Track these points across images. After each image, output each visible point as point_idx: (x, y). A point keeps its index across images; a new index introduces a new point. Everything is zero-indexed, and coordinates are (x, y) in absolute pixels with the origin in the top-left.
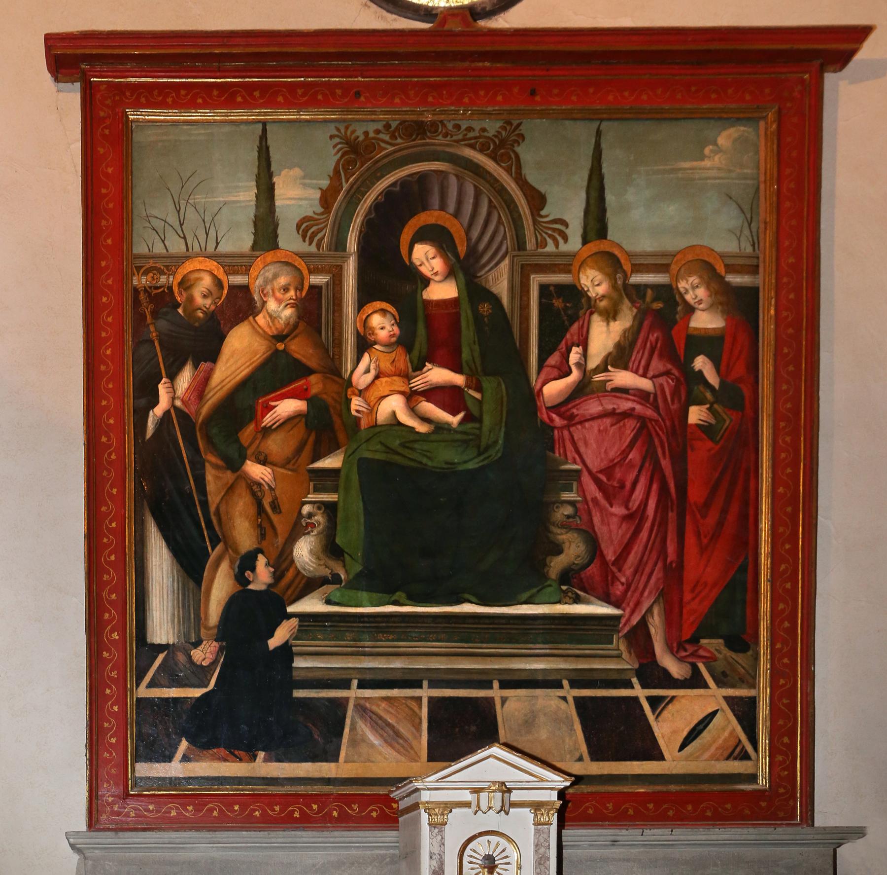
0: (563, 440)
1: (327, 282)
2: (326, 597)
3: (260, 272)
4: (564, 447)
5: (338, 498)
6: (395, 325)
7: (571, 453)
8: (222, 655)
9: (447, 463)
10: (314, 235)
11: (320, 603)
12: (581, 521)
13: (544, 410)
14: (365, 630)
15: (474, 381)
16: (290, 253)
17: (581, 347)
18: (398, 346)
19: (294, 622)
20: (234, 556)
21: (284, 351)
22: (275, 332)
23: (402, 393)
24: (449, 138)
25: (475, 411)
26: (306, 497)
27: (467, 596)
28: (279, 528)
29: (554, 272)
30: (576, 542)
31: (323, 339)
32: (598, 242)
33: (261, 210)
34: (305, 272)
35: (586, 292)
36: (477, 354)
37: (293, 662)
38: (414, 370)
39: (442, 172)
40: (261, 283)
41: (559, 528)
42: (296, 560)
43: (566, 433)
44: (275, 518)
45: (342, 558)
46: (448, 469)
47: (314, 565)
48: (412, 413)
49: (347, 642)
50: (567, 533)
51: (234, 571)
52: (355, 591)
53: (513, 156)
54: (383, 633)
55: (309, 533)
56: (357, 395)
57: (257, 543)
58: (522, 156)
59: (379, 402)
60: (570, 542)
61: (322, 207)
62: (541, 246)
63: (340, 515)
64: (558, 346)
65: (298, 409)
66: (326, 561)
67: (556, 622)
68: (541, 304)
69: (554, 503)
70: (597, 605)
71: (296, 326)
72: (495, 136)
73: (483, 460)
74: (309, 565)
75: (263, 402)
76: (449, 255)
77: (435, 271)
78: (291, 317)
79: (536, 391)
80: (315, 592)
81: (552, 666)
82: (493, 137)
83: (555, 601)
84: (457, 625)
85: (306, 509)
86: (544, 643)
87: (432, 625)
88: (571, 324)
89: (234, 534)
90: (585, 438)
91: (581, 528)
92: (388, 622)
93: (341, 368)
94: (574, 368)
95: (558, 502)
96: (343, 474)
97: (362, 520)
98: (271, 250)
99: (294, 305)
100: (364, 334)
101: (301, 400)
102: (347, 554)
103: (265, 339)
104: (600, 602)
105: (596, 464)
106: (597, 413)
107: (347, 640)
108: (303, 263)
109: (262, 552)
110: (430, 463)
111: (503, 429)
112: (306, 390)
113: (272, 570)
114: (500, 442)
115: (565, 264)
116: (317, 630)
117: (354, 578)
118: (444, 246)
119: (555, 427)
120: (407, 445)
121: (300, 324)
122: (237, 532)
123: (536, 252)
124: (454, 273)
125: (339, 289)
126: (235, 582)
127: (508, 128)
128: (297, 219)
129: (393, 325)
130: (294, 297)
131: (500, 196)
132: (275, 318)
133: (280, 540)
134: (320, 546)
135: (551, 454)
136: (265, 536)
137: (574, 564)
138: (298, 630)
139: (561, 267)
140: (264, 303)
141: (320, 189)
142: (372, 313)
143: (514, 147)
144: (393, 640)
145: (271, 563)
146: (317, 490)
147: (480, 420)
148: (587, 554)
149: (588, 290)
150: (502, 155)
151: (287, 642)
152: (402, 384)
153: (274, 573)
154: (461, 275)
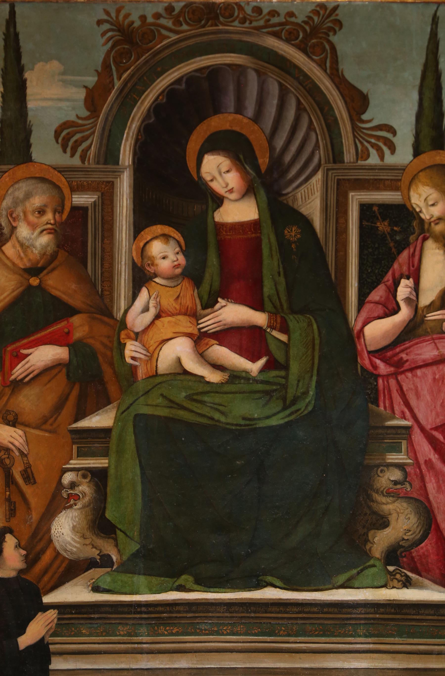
0: (390, 391)
1: (95, 202)
2: (94, 582)
3: (7, 191)
4: (391, 398)
5: (109, 463)
6: (181, 254)
7: (398, 406)
9: (244, 419)
10: (77, 144)
11: (86, 590)
12: (411, 488)
13: (366, 355)
14: (143, 622)
15: (279, 320)
16: (47, 167)
17: (411, 280)
18: (184, 279)
19: (52, 614)
21: (40, 287)
22: (28, 265)
23: (189, 335)
24: (247, 25)
25: (280, 356)
26: (68, 463)
27: (269, 579)
28: (33, 501)
29: (378, 189)
30: (406, 512)
31: (90, 274)
32: (434, 153)
33: (9, 113)
34: (66, 191)
35: (418, 213)
36: (282, 288)
37: (50, 664)
38: (204, 307)
39: (239, 66)
40: (9, 204)
41: (384, 496)
42: (54, 539)
43: (392, 382)
44: (27, 490)
45: (113, 535)
46: (245, 425)
47: (78, 545)
48: (201, 359)
49: (119, 638)
50: (394, 502)
52: (131, 575)
53: (327, 47)
54: (165, 625)
55: (71, 507)
56: (133, 339)
58: (339, 48)
59: (160, 346)
60: (398, 513)
61: (88, 109)
62: (362, 157)
63: (111, 484)
64: (383, 277)
65: (57, 357)
66: (92, 540)
67: (382, 610)
68: (361, 228)
69: (378, 466)
70: (433, 590)
71: (54, 257)
72: (305, 22)
73: (290, 415)
74: (70, 544)
75: (13, 350)
76: (248, 168)
77: (230, 187)
78: (47, 245)
79: (355, 332)
81: (377, 664)
82: (303, 24)
83: (380, 584)
84: (258, 615)
85: (68, 478)
86: (366, 636)
87: (226, 615)
88: (400, 252)
90: (416, 388)
91: (412, 496)
92: (171, 612)
93: (112, 307)
94: (403, 305)
95: (382, 466)
96: (114, 434)
97: (139, 488)
98: (23, 163)
99: (53, 231)
100: (142, 265)
101: (61, 346)
102: (121, 530)
103: (15, 273)
104: (437, 587)
105: (430, 420)
106: (432, 359)
107: (120, 635)
108: (63, 180)
109: (11, 532)
110: (223, 419)
111: (315, 378)
112: (68, 333)
113: (24, 552)
114: (311, 393)
115: (392, 180)
116: (81, 624)
117: (129, 559)
118: (241, 157)
119: (379, 376)
120: (195, 397)
121: (59, 253)
123: (357, 164)
124: (253, 189)
125: (110, 210)
127: (322, 12)
128: (55, 126)
129: (178, 253)
130: (52, 222)
131: (311, 96)
132: (28, 247)
133: (35, 516)
134: (85, 522)
135: (372, 406)
136: (15, 512)
137: (403, 539)
139: (387, 183)
140: (13, 229)
141: (85, 87)
142: (151, 240)
143: (329, 36)
144: (177, 634)
145: (23, 543)
146: (81, 454)
147: (286, 367)
148: (420, 527)
149: (421, 211)
150: (314, 46)
151: (43, 639)
152: (189, 325)
153: (26, 556)
154: (262, 193)
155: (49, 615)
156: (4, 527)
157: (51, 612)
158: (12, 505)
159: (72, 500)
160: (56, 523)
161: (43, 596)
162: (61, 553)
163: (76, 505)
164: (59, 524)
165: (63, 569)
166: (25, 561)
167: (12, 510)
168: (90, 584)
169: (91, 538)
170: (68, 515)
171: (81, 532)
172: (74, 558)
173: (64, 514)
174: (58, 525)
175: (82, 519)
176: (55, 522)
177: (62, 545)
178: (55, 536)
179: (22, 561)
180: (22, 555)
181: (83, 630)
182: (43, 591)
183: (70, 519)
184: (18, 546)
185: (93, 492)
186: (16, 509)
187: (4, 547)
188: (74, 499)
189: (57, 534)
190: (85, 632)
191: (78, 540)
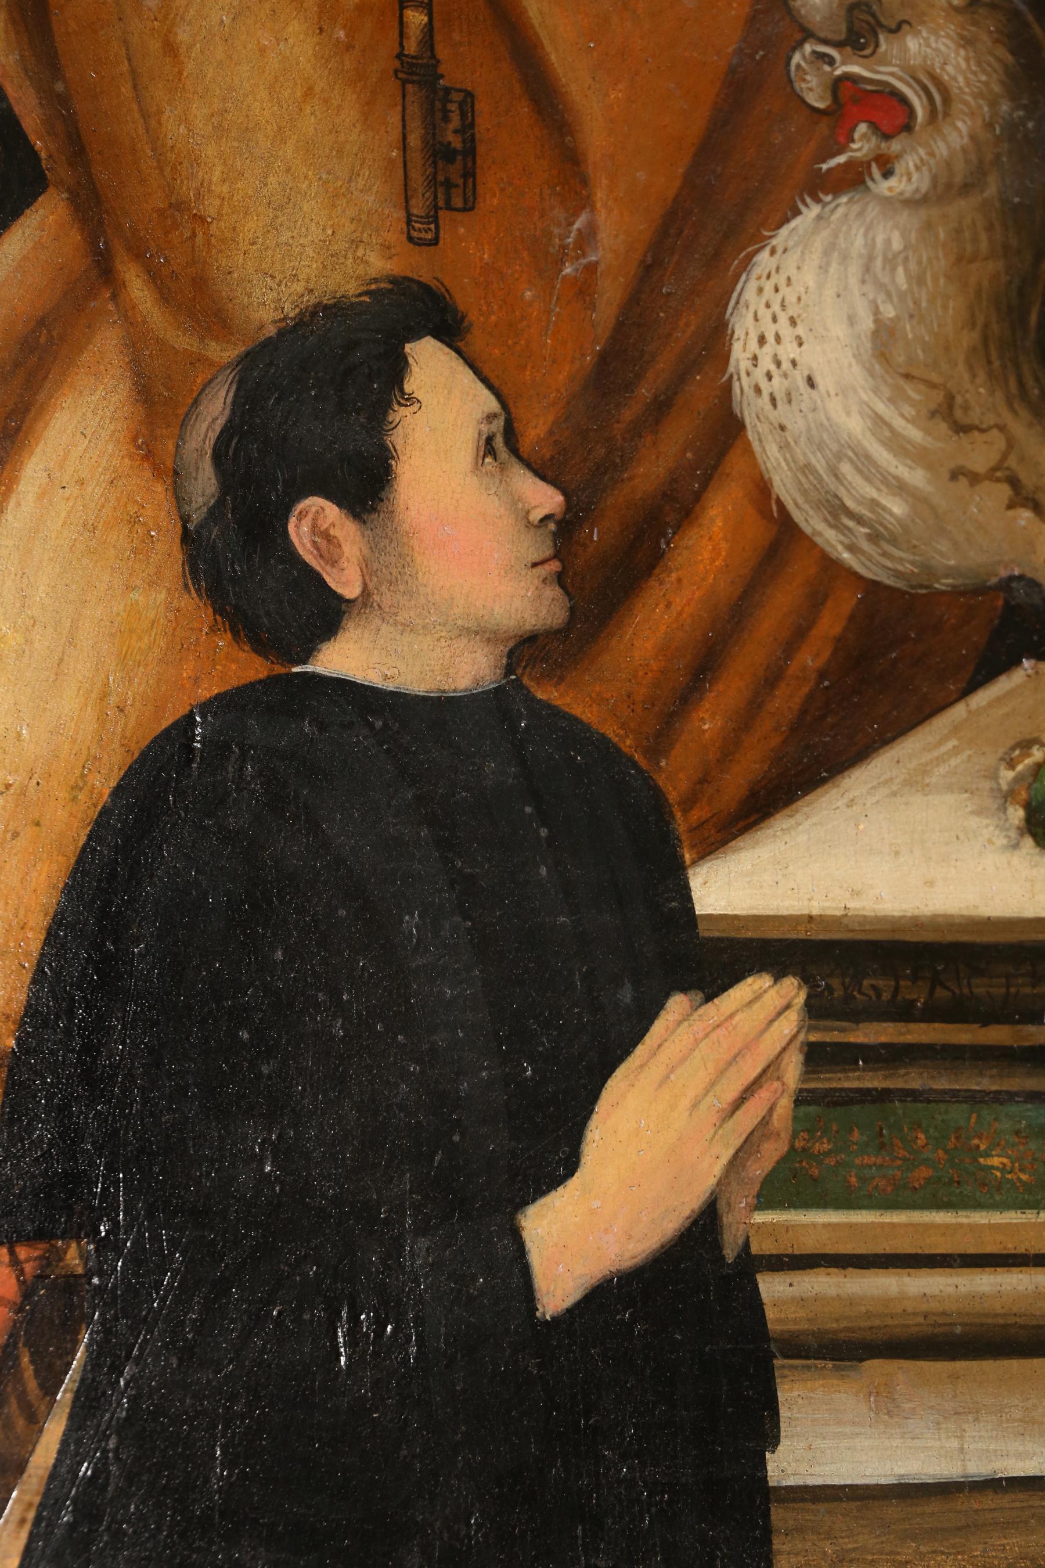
8: (50, 1389)
11: (986, 828)
20: (184, 341)
37: (773, 1440)
51: (179, 498)
57: (395, 236)
66: (1011, 443)
74: (865, 464)
80: (942, 722)
89: (173, 130)
116: (974, 1099)
122: (199, 112)
126: (191, 603)
136: (470, 174)
138: (802, 1099)
155: (748, 1022)
156: (394, 280)
157: (757, 998)
158: (446, 119)
159: (862, 128)
160: (760, 290)
161: (694, 863)
162: (808, 531)
163: (887, 174)
164: (783, 306)
165: (827, 654)
166: (555, 566)
167: (448, 154)
168: (1017, 779)
169: (1002, 428)
170: (841, 240)
171: (934, 377)
172: (898, 574)
173: (815, 231)
174: (776, 307)
175: (935, 279)
176: (752, 285)
177: (807, 468)
178: (758, 390)
179: (535, 565)
180: (536, 515)
181: (987, 1155)
182: (697, 815)
183: (854, 270)
184: (499, 442)
185: (997, 88)
186: (481, 149)
187: (396, 439)
188: (874, 126)
189: (769, 376)
190: (1003, 1169)
191: (915, 434)
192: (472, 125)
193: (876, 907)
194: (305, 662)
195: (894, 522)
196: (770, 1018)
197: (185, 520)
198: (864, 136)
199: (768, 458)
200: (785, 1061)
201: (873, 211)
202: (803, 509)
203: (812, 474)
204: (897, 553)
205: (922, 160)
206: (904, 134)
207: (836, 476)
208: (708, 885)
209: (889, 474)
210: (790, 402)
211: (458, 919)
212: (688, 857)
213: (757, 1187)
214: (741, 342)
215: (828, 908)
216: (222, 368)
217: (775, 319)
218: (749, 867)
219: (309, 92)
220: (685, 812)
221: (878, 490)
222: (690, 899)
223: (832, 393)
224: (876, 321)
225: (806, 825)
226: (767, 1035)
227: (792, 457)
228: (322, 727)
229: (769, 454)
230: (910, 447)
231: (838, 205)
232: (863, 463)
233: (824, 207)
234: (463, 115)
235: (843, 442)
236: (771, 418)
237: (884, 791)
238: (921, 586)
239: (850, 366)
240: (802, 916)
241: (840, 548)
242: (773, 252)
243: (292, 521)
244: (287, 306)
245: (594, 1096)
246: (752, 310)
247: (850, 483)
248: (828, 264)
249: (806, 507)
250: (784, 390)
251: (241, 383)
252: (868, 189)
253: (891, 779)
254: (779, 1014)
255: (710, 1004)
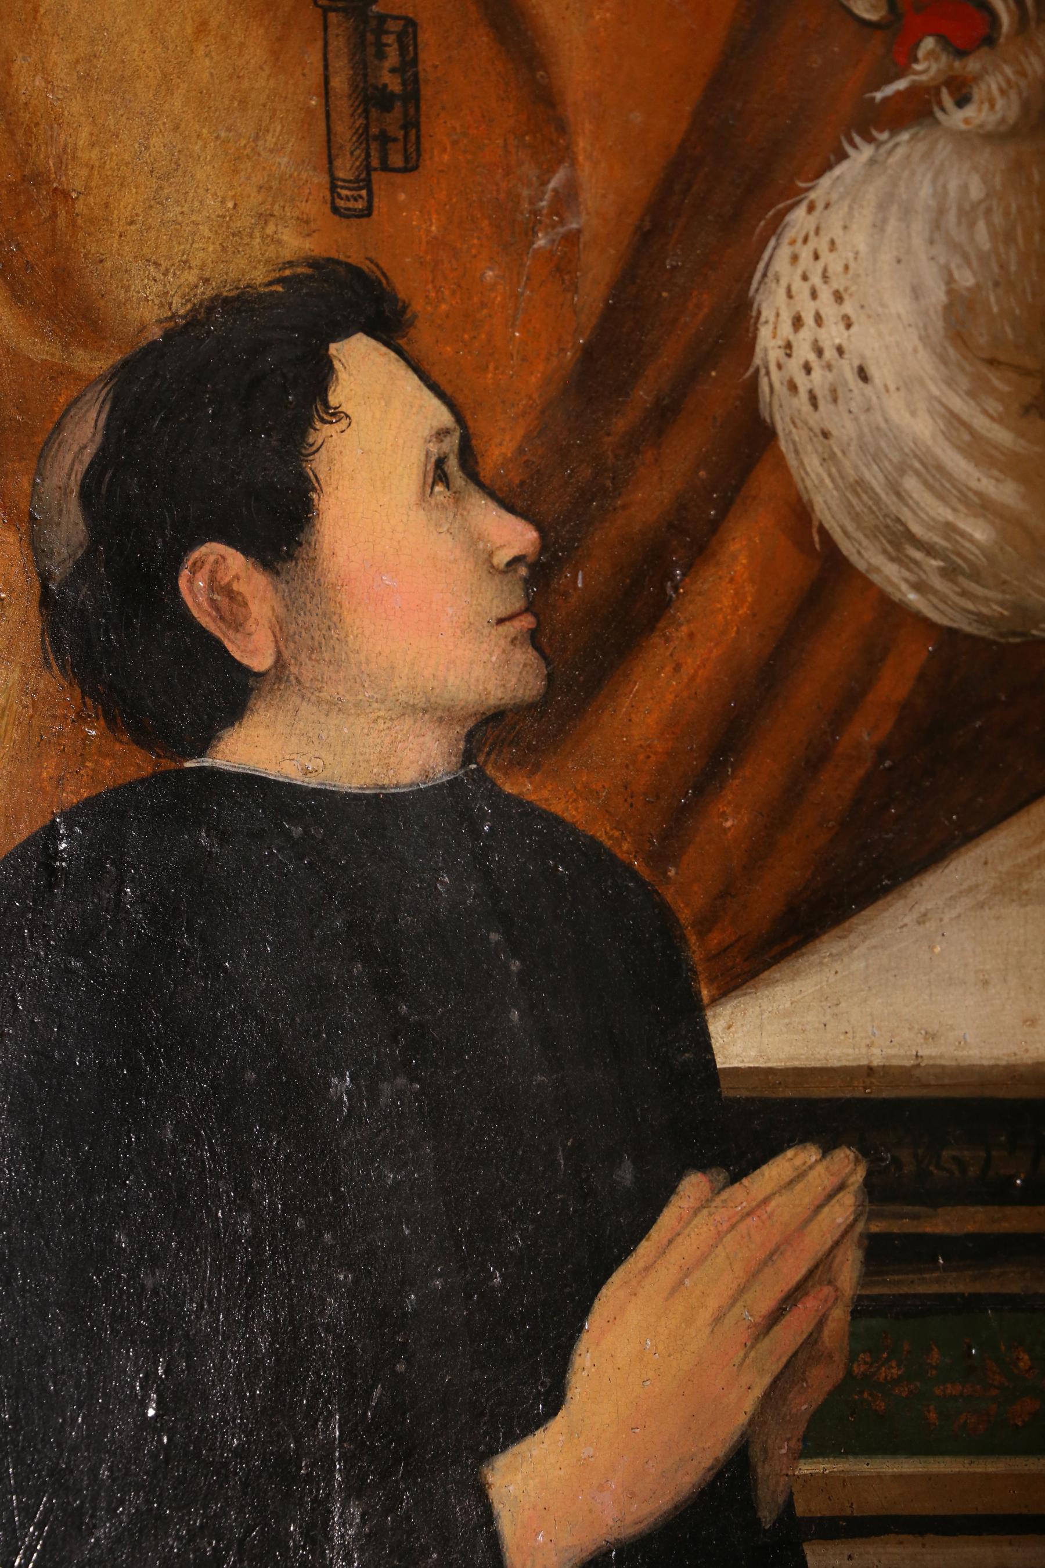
57: (315, 207)
122: (60, 59)
136: (412, 124)
156: (314, 263)
157: (800, 1176)
158: (381, 55)
159: (929, 43)
160: (795, 258)
161: (714, 1001)
162: (861, 566)
163: (962, 102)
164: (825, 277)
166: (527, 622)
167: (383, 100)
172: (981, 619)
174: (816, 279)
176: (784, 252)
177: (859, 486)
178: (793, 387)
179: (500, 621)
180: (502, 558)
182: (716, 939)
183: (920, 226)
184: (453, 466)
187: (319, 465)
188: (945, 41)
189: (808, 369)
191: (1002, 436)
192: (415, 61)
193: (959, 1053)
194: (201, 754)
195: (977, 552)
196: (817, 1203)
197: (45, 578)
198: (931, 55)
199: (807, 473)
200: (838, 1260)
201: (944, 150)
202: (855, 540)
203: (866, 493)
204: (979, 591)
205: (1008, 81)
206: (985, 49)
207: (898, 494)
208: (733, 1029)
209: (970, 489)
210: (835, 400)
211: (401, 1081)
212: (705, 993)
213: (802, 1427)
214: (771, 326)
215: (894, 1056)
216: (93, 383)
217: (814, 295)
218: (788, 1005)
219: (202, 28)
220: (702, 935)
221: (955, 510)
222: (708, 1048)
223: (892, 387)
224: (949, 292)
225: (863, 948)
226: (814, 1226)
227: (839, 472)
228: (224, 838)
229: (809, 469)
230: (997, 454)
231: (897, 145)
232: (933, 476)
233: (878, 147)
234: (403, 49)
235: (906, 450)
236: (811, 423)
237: (968, 901)
238: (1014, 634)
239: (915, 351)
240: (859, 1067)
241: (904, 587)
242: (811, 208)
243: (185, 573)
244: (176, 302)
245: (585, 1310)
246: (784, 283)
247: (917, 503)
248: (884, 221)
249: (859, 535)
250: (827, 386)
251: (117, 401)
252: (937, 122)
253: (977, 886)
254: (830, 1197)
255: (737, 1185)
